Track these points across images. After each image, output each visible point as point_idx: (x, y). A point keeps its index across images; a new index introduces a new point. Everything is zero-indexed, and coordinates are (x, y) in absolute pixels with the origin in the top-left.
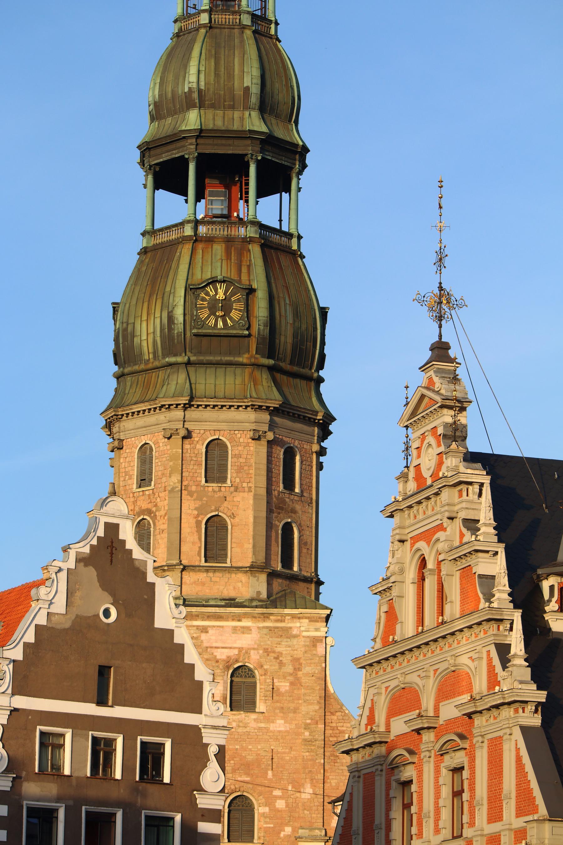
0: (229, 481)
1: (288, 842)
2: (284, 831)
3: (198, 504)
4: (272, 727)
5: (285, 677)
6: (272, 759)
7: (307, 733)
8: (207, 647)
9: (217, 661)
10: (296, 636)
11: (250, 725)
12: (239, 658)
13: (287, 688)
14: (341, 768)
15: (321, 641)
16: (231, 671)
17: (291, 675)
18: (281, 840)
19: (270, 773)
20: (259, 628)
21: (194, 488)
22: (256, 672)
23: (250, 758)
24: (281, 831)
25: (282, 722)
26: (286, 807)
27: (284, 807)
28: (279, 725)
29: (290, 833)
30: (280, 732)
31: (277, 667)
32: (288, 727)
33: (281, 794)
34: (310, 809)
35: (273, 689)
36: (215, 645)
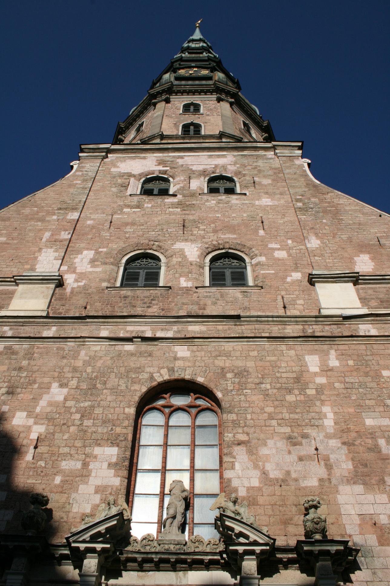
0: (201, 111)
1: (299, 286)
2: (291, 276)
3: (176, 120)
4: (257, 203)
5: (265, 177)
6: (262, 222)
7: (300, 204)
8: (182, 165)
9: (193, 171)
10: (271, 159)
11: (233, 202)
12: (216, 170)
13: (270, 182)
14: (350, 227)
15: (298, 159)
16: (207, 178)
17: (272, 176)
18: (288, 285)
19: (261, 232)
20: (233, 155)
21: (173, 115)
22: (234, 178)
23: (235, 222)
24: (287, 276)
25: (270, 200)
26: (288, 257)
27: (286, 256)
28: (266, 201)
29: (300, 278)
30: (268, 206)
31: (256, 172)
32: (276, 203)
33: (279, 247)
34: (322, 255)
35: (254, 183)
36: (190, 163)
